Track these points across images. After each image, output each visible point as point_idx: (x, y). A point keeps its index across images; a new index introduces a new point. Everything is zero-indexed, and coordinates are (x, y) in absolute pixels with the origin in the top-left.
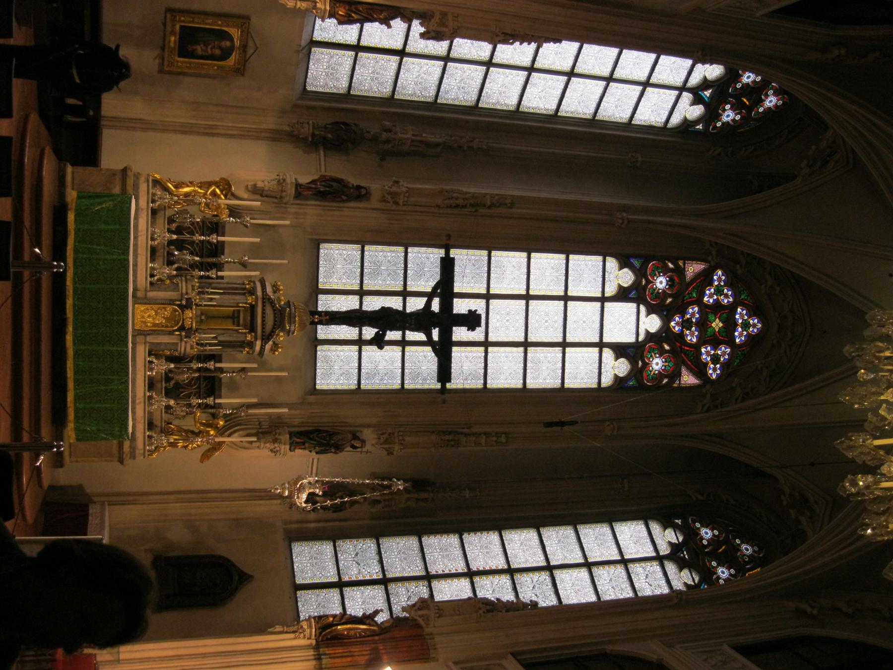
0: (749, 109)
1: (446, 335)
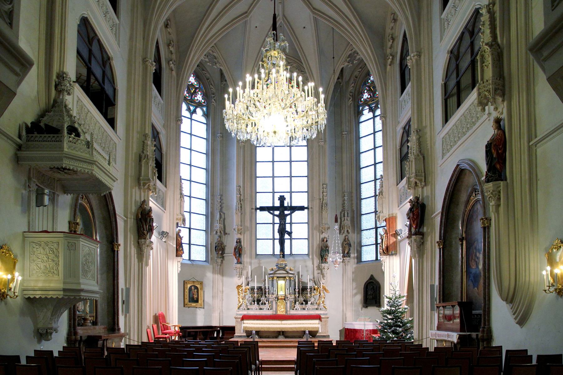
0: (196, 89)
1: (286, 208)
